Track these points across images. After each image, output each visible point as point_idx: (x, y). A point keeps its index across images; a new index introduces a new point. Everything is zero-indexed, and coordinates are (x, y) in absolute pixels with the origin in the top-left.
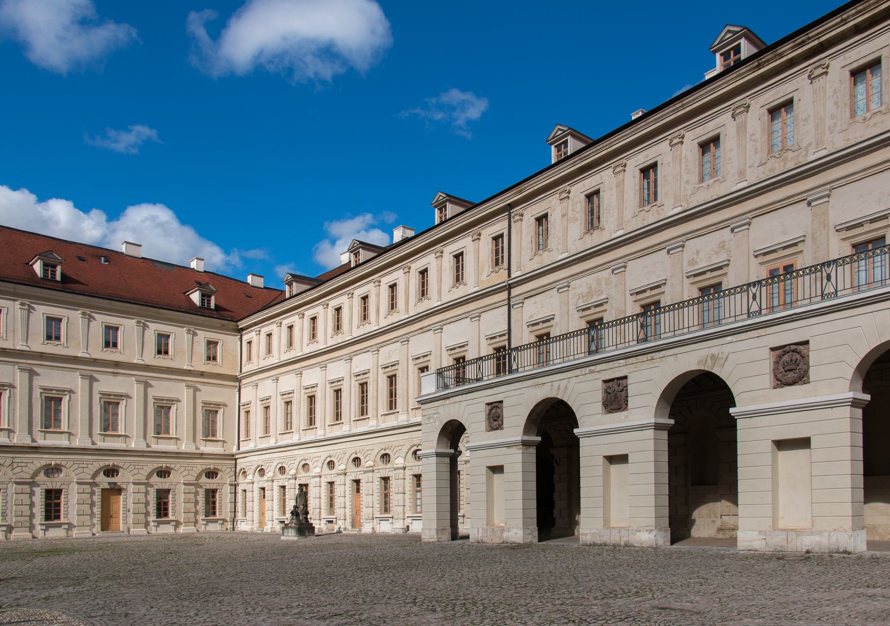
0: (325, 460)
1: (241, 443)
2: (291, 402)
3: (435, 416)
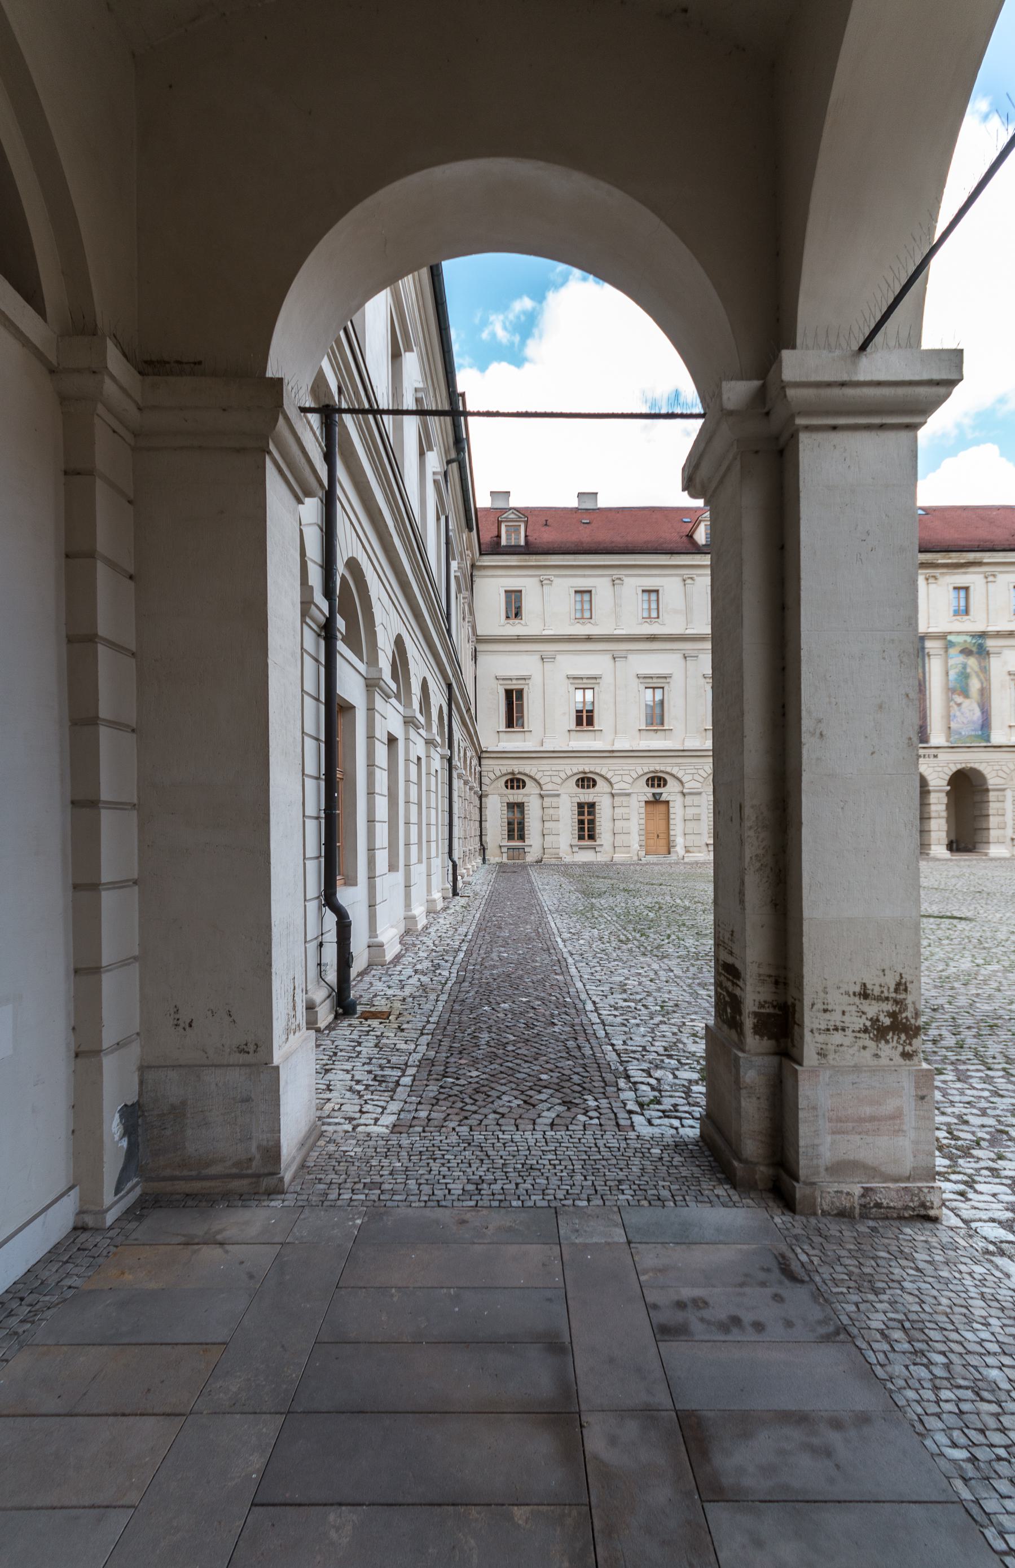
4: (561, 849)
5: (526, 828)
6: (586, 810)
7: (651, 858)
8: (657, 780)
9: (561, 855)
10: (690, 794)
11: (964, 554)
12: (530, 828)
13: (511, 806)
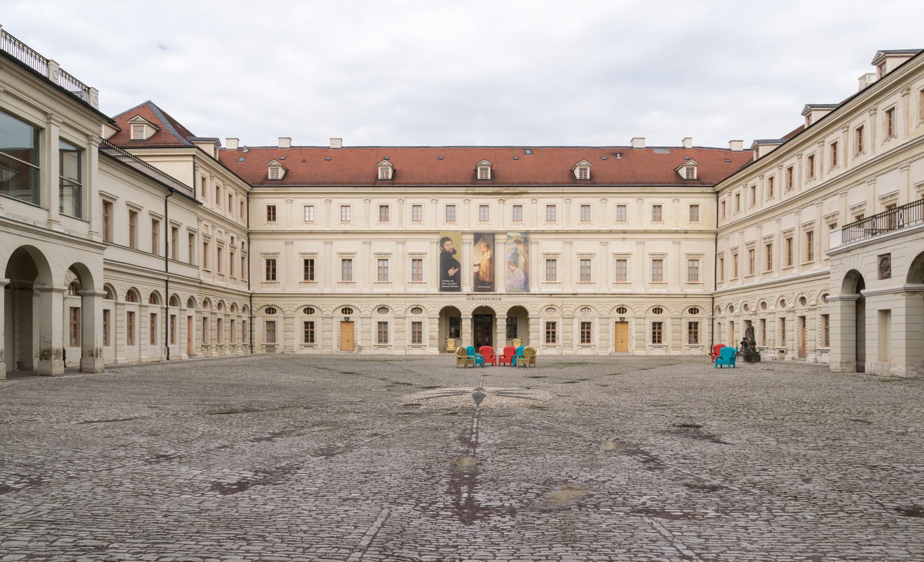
0: (778, 299)
1: (717, 286)
2: (753, 250)
3: (840, 266)
8: (347, 310)
9: (295, 350)
10: (364, 318)
13: (268, 323)
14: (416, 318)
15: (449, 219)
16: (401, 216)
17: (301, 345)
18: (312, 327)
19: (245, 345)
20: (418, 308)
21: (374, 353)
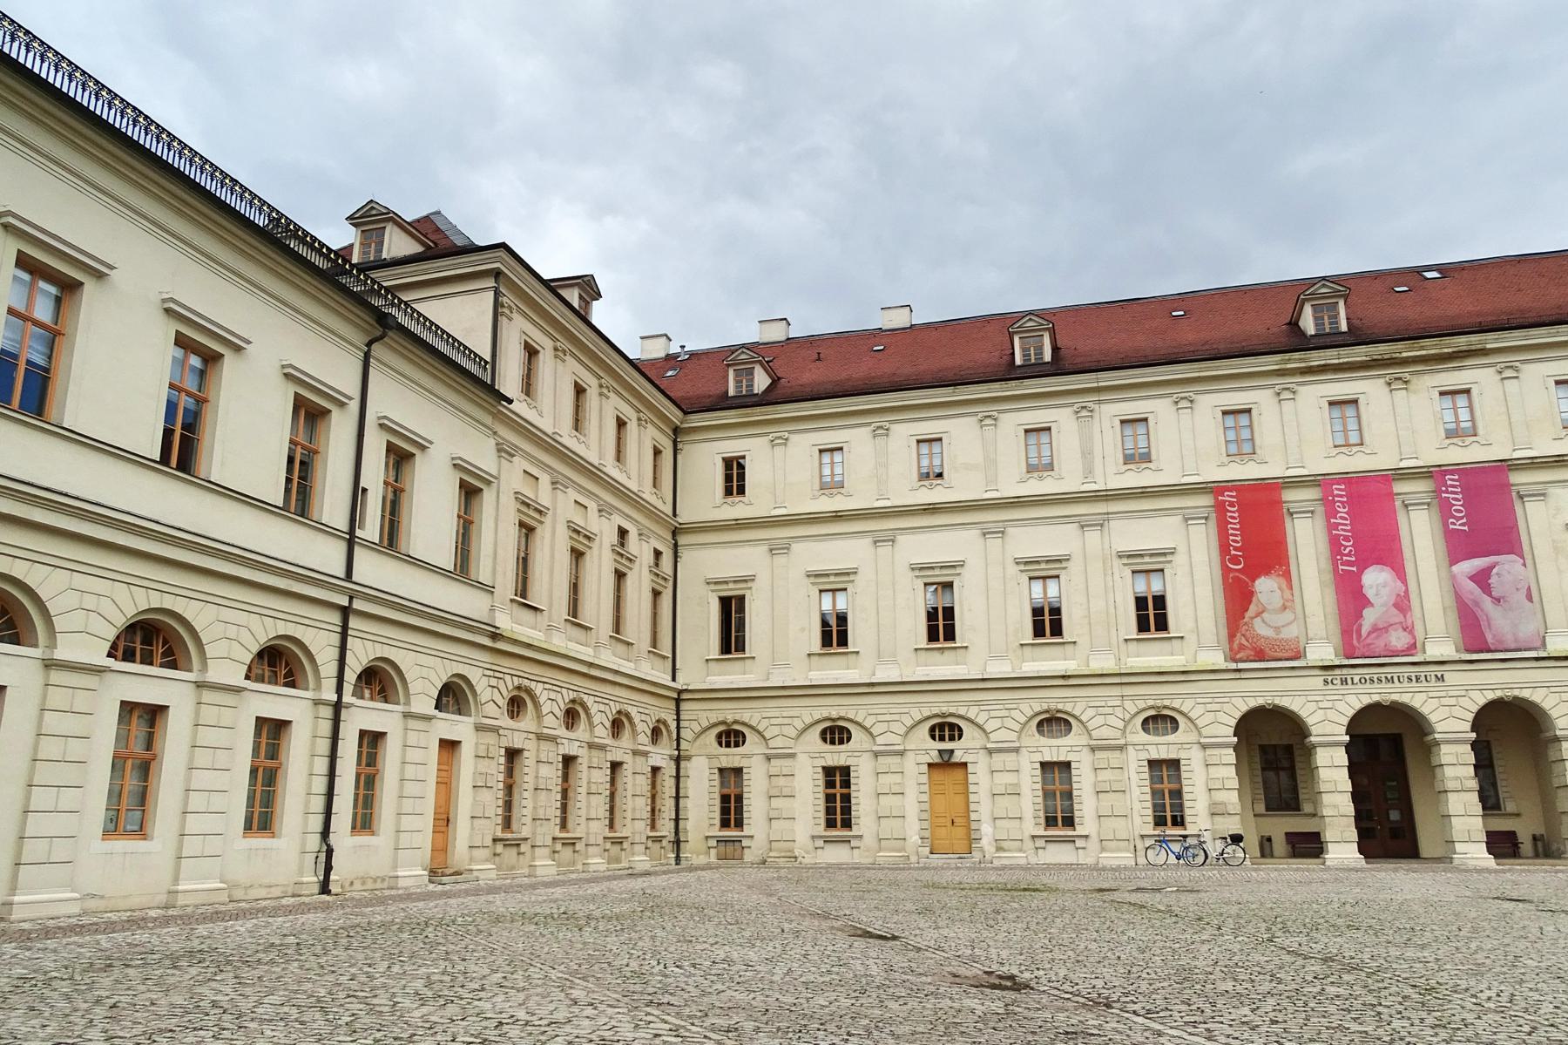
4: (797, 845)
5: (745, 808)
6: (838, 779)
7: (936, 860)
8: (946, 730)
10: (1000, 750)
11: (1447, 340)
12: (751, 808)
14: (1162, 746)
15: (1233, 449)
16: (1087, 454)
17: (813, 837)
18: (847, 784)
19: (658, 839)
20: (1165, 717)
21: (1033, 860)
